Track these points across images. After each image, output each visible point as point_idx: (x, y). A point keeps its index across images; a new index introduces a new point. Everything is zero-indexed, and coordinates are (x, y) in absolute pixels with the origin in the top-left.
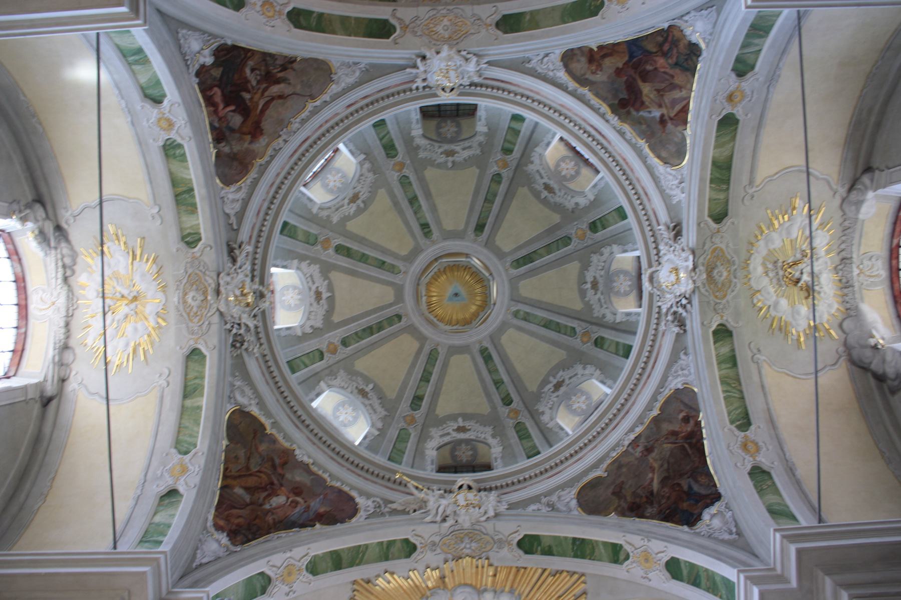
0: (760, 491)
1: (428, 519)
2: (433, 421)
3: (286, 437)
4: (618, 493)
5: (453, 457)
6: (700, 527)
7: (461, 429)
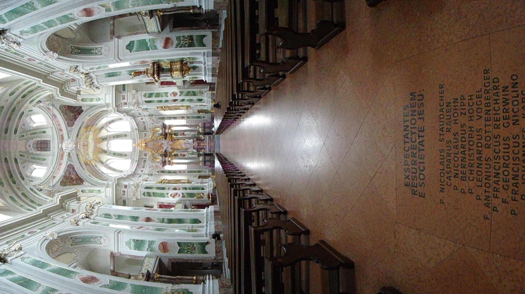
0: (86, 101)
1: (73, 152)
2: (27, 152)
3: (61, 177)
4: (71, 120)
5: (36, 148)
6: (84, 110)
7: (30, 146)
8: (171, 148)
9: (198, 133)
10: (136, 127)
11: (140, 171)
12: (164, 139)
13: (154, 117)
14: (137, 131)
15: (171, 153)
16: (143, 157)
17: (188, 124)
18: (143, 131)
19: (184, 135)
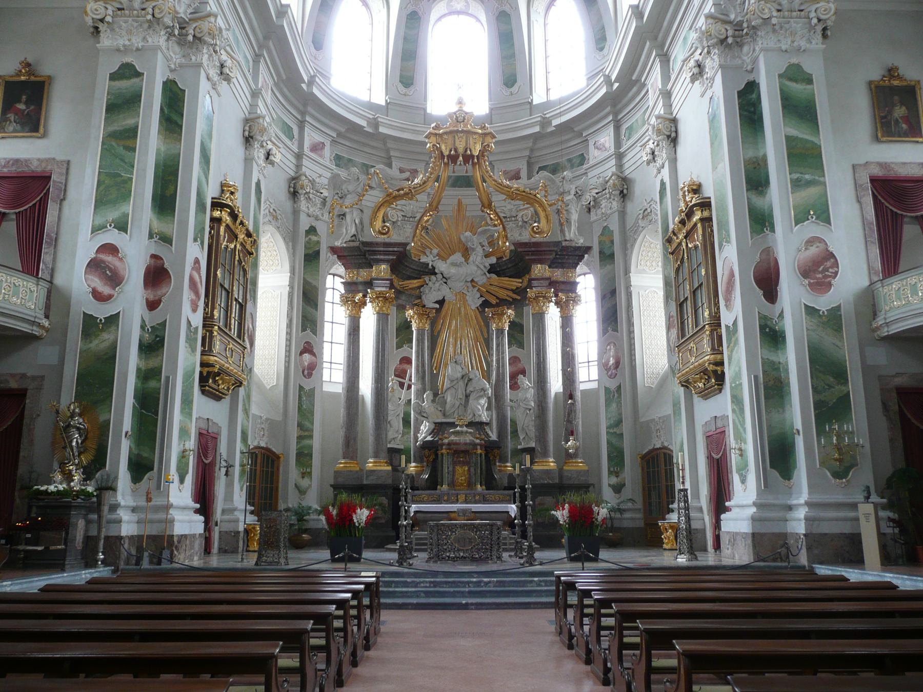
8: (441, 302)
9: (530, 451)
10: (555, 122)
11: (318, 138)
12: (493, 260)
13: (615, 205)
14: (537, 129)
15: (416, 299)
16: (396, 164)
17: (578, 395)
18: (530, 165)
19: (513, 377)
